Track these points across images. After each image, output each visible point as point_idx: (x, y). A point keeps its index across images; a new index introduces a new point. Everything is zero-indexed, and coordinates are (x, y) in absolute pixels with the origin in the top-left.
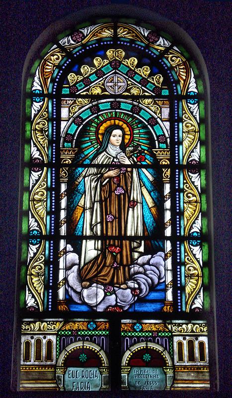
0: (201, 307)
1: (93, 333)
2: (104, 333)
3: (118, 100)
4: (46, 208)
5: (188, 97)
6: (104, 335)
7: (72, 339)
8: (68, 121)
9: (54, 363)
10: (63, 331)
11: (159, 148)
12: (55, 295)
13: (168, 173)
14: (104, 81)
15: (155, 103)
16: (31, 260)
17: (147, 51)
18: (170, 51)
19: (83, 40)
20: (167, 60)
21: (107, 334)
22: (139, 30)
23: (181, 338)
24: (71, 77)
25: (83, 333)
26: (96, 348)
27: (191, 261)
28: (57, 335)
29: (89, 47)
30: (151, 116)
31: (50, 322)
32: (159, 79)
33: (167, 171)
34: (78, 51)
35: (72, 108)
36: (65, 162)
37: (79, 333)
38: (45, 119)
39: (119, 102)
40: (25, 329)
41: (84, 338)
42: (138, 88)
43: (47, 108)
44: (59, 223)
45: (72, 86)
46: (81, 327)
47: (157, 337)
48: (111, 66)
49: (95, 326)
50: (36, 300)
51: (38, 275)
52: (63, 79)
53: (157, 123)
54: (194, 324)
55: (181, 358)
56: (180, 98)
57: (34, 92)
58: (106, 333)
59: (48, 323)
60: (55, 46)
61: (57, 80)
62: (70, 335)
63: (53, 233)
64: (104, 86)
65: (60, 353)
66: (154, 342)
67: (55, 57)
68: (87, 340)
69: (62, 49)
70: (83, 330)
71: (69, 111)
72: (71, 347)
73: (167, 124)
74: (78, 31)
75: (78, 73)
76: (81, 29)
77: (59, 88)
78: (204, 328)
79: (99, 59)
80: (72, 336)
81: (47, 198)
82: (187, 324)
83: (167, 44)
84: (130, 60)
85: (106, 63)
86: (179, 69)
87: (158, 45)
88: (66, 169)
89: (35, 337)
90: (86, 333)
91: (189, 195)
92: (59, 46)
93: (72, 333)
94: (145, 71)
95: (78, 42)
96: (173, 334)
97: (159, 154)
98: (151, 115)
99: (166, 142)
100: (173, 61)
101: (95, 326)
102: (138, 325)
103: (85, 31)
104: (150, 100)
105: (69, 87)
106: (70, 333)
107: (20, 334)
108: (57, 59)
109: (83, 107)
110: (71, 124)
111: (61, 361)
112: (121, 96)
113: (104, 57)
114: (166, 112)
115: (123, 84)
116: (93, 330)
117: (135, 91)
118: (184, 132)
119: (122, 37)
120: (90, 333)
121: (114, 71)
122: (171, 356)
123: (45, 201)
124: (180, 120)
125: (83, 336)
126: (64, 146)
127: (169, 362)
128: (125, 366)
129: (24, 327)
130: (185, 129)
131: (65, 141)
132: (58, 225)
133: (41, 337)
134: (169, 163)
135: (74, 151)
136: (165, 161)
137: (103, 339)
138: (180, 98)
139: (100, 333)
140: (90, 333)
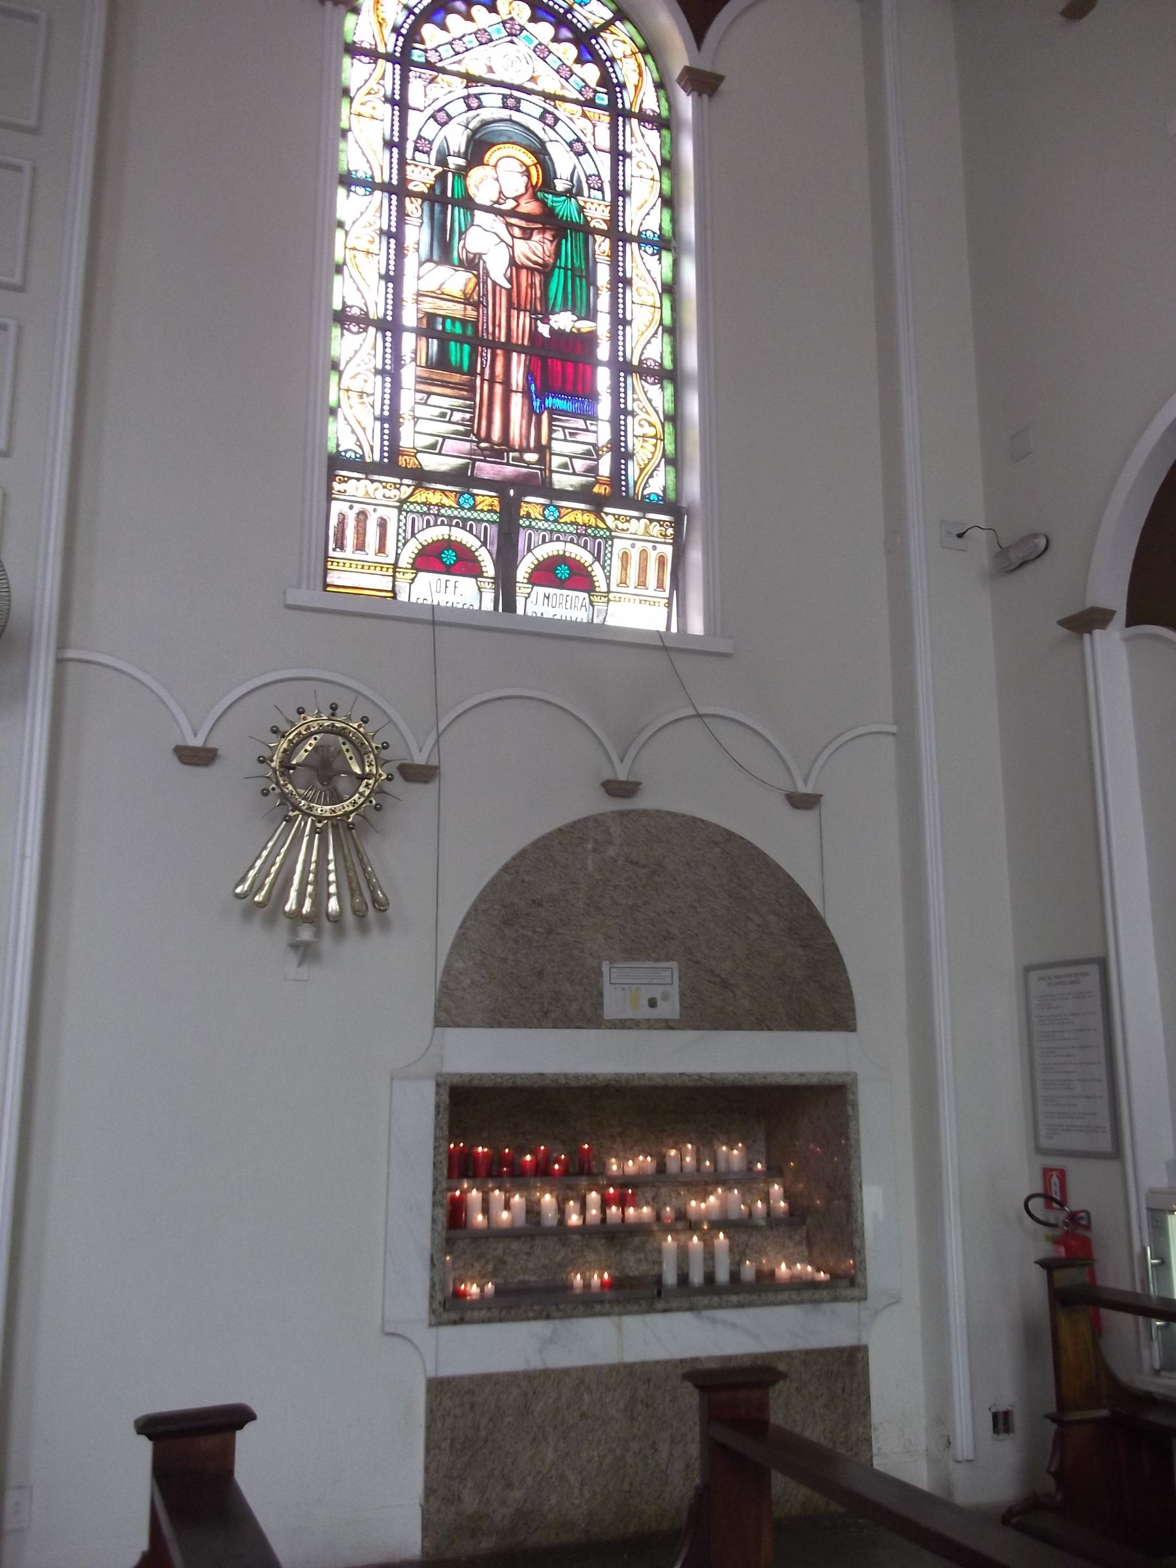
0: (662, 495)
1: (469, 514)
6: (488, 521)
10: (412, 503)
11: (589, 197)
15: (584, 115)
23: (627, 544)
24: (429, 31)
27: (644, 410)
32: (591, 73)
39: (518, 100)
41: (450, 521)
47: (585, 535)
53: (586, 151)
56: (627, 115)
62: (425, 513)
68: (457, 525)
70: (450, 507)
75: (443, 27)
77: (407, 49)
80: (429, 514)
82: (638, 519)
94: (569, 52)
96: (613, 534)
99: (601, 189)
102: (552, 508)
106: (425, 509)
111: (406, 559)
112: (520, 89)
120: (462, 513)
124: (627, 155)
125: (450, 518)
126: (414, 159)
127: (601, 585)
133: (370, 508)
135: (432, 170)
137: (486, 528)
138: (627, 115)
140: (462, 513)
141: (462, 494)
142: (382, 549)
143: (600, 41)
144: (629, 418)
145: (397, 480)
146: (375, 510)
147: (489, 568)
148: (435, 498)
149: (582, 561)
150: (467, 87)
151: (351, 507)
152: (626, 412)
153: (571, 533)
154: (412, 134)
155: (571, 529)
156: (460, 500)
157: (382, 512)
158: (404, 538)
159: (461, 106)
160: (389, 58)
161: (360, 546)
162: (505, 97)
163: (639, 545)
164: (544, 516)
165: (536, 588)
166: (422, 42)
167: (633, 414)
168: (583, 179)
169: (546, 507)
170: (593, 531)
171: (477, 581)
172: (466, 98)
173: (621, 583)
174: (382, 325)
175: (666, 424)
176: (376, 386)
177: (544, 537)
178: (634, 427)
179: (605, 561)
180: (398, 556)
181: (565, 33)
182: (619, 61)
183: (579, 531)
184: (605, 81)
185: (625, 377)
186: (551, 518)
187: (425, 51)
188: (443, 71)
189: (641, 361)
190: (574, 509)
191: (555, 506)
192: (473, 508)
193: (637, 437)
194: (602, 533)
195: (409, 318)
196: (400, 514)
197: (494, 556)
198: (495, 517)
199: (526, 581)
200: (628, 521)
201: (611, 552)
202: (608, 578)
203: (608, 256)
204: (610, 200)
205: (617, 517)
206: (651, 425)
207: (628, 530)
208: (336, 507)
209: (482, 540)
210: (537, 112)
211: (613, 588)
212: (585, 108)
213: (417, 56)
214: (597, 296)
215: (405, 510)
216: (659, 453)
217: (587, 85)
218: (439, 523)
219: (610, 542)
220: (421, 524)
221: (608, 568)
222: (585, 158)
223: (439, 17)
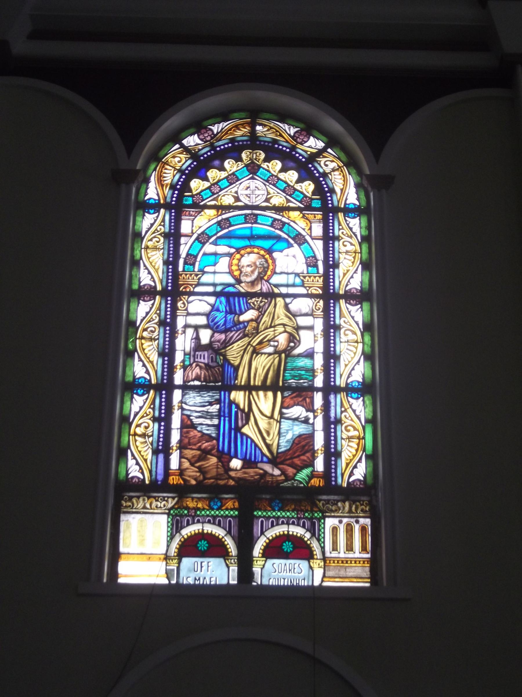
1: (217, 513)
2: (232, 513)
5: (347, 211)
6: (231, 516)
7: (188, 521)
8: (191, 236)
14: (238, 188)
15: (304, 216)
16: (135, 416)
17: (294, 153)
18: (324, 154)
20: (319, 164)
21: (236, 516)
22: (284, 128)
26: (219, 532)
28: (169, 514)
31: (159, 497)
32: (308, 187)
33: (318, 302)
38: (160, 234)
39: (256, 215)
43: (163, 220)
45: (197, 195)
46: (200, 505)
47: (304, 518)
49: (219, 504)
51: (144, 435)
52: (185, 187)
53: (306, 241)
55: (335, 548)
56: (336, 210)
57: (148, 201)
58: (234, 513)
60: (177, 146)
61: (178, 187)
62: (186, 515)
63: (165, 381)
66: (298, 525)
67: (177, 159)
69: (186, 149)
74: (206, 128)
75: (206, 179)
77: (180, 197)
78: (366, 507)
80: (189, 516)
83: (321, 145)
87: (309, 147)
88: (185, 298)
90: (208, 513)
91: (347, 332)
92: (182, 146)
97: (308, 281)
99: (316, 266)
100: (326, 165)
101: (219, 504)
103: (215, 129)
105: (192, 196)
108: (179, 162)
113: (239, 159)
114: (318, 229)
115: (263, 192)
116: (217, 510)
119: (263, 137)
120: (213, 513)
121: (251, 175)
122: (320, 545)
127: (317, 552)
128: (258, 557)
130: (343, 249)
131: (185, 263)
132: (171, 369)
136: (315, 290)
137: (230, 521)
139: (227, 513)
143: (316, 165)
154: (183, 254)
163: (345, 520)
166: (190, 191)
174: (158, 388)
177: (272, 522)
178: (342, 433)
179: (319, 535)
182: (329, 175)
183: (299, 516)
187: (192, 196)
196: (168, 517)
198: (236, 513)
199: (260, 555)
201: (324, 528)
204: (322, 273)
206: (355, 429)
209: (227, 529)
210: (269, 221)
211: (328, 555)
212: (304, 212)
215: (172, 515)
217: (306, 196)
218: (196, 521)
219: (322, 521)
221: (322, 540)
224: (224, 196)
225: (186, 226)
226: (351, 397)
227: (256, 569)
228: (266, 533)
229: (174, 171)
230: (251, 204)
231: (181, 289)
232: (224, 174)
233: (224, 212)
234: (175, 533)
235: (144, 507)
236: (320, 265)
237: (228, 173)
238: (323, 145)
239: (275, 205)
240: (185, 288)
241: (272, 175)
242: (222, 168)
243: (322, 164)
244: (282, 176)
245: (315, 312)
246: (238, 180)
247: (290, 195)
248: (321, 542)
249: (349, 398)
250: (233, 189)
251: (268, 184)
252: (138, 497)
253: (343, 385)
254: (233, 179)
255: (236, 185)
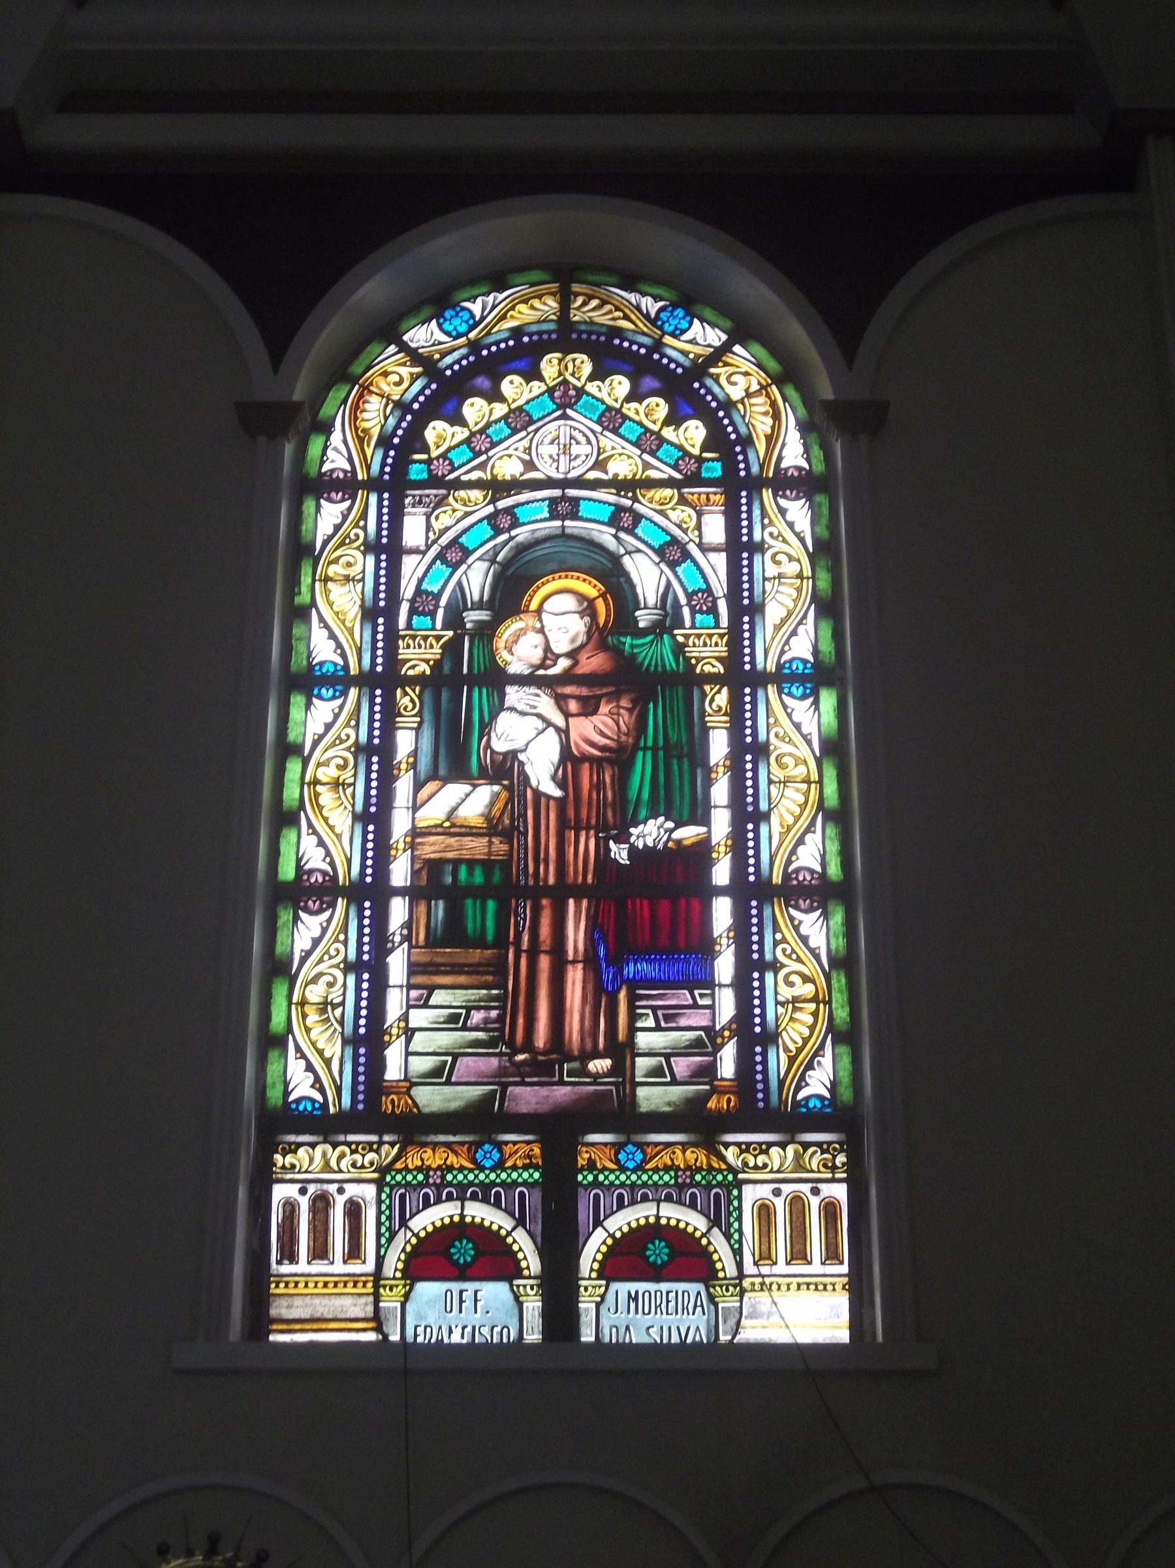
0: (827, 1095)
1: (493, 1176)
2: (525, 1175)
3: (572, 492)
4: (353, 806)
6: (525, 1183)
9: (370, 1266)
10: (399, 1171)
11: (693, 627)
12: (376, 1064)
13: (722, 698)
15: (683, 501)
19: (471, 329)
20: (717, 380)
21: (536, 1181)
23: (765, 1191)
24: (437, 432)
25: (460, 1177)
27: (794, 956)
28: (380, 1184)
29: (489, 349)
30: (669, 538)
31: (358, 1144)
32: (694, 433)
33: (719, 692)
34: (458, 362)
35: (437, 518)
36: (411, 672)
37: (449, 1177)
39: (575, 501)
40: (283, 1167)
41: (462, 1194)
42: (629, 457)
43: (364, 515)
44: (392, 767)
46: (453, 1160)
47: (691, 1186)
48: (552, 398)
50: (339, 645)
52: (413, 441)
53: (686, 555)
54: (806, 1146)
59: (353, 1147)
60: (392, 349)
62: (421, 1185)
64: (530, 454)
65: (390, 1241)
66: (680, 1202)
68: (474, 1197)
70: (461, 1169)
71: (429, 527)
72: (426, 1220)
73: (720, 560)
75: (457, 419)
76: (468, 300)
79: (517, 379)
80: (428, 1185)
81: (355, 775)
82: (783, 1145)
83: (716, 337)
84: (608, 381)
85: (536, 392)
86: (751, 405)
87: (689, 342)
88: (414, 691)
89: (312, 1189)
90: (471, 1177)
92: (404, 347)
93: (427, 1177)
95: (459, 336)
96: (740, 1176)
98: (668, 533)
99: (713, 610)
100: (735, 384)
102: (630, 1148)
103: (476, 308)
104: (668, 492)
106: (420, 1177)
107: (264, 1179)
109: (467, 514)
110: (433, 562)
111: (394, 1262)
112: (580, 483)
113: (532, 374)
114: (715, 528)
117: (621, 468)
118: (769, 579)
120: (482, 1176)
122: (732, 1247)
123: (349, 785)
129: (278, 1158)
132: (382, 855)
133: (332, 1188)
134: (722, 671)
135: (438, 638)
137: (522, 1194)
138: (755, 484)
140: (482, 1176)
141: (479, 1145)
142: (354, 1251)
143: (709, 382)
144: (769, 977)
145: (374, 1138)
146: (341, 1191)
147: (532, 1262)
148: (434, 1159)
149: (690, 1229)
150: (493, 501)
151: (303, 1191)
152: (764, 966)
153: (666, 1185)
154: (407, 589)
155: (666, 1178)
156: (478, 1156)
157: (352, 1190)
158: (389, 1229)
159: (486, 530)
160: (373, 485)
161: (320, 1251)
162: (553, 502)
163: (787, 1188)
164: (617, 1162)
165: (615, 1286)
166: (426, 449)
167: (775, 966)
168: (683, 600)
169: (618, 1147)
170: (703, 1177)
171: (511, 1286)
172: (492, 519)
173: (761, 1258)
174: (356, 893)
175: (834, 975)
176: (346, 990)
177: (621, 1196)
179: (730, 1225)
180: (380, 1261)
181: (649, 382)
182: (740, 406)
184: (717, 440)
185: (760, 908)
186: (631, 1165)
188: (458, 484)
189: (786, 876)
190: (668, 1145)
191: (634, 1144)
192: (499, 1166)
193: (782, 1004)
194: (720, 1177)
195: (400, 873)
197: (539, 1239)
198: (537, 1175)
200: (766, 1152)
201: (740, 1208)
202: (738, 1253)
203: (725, 714)
205: (745, 1148)
206: (806, 979)
207: (765, 1166)
208: (280, 1192)
210: (606, 513)
211: (749, 1268)
213: (417, 472)
214: (709, 783)
215: (388, 1184)
216: (822, 1026)
217: (686, 454)
218: (444, 1197)
219: (735, 1192)
220: (414, 1204)
221: (736, 1236)
222: (684, 569)
223: (450, 406)
224: (501, 458)
225: (413, 530)
226: (790, 694)
227: (586, 1305)
228: (606, 1224)
229: (387, 405)
230: (561, 476)
231: (403, 673)
232: (500, 409)
233: (498, 496)
234: (397, 1228)
235: (327, 1168)
236: (722, 606)
237: (509, 405)
238: (724, 337)
239: (616, 475)
240: (413, 667)
241: (609, 409)
242: (495, 396)
243: (723, 380)
244: (630, 409)
245: (710, 715)
246: (531, 422)
247: (653, 453)
248: (732, 1242)
249: (783, 696)
250: (518, 443)
251: (598, 429)
252: (313, 1146)
253: (771, 667)
254: (519, 420)
255: (528, 434)
